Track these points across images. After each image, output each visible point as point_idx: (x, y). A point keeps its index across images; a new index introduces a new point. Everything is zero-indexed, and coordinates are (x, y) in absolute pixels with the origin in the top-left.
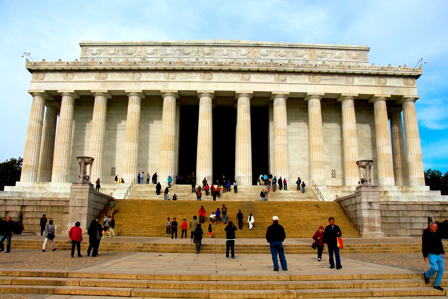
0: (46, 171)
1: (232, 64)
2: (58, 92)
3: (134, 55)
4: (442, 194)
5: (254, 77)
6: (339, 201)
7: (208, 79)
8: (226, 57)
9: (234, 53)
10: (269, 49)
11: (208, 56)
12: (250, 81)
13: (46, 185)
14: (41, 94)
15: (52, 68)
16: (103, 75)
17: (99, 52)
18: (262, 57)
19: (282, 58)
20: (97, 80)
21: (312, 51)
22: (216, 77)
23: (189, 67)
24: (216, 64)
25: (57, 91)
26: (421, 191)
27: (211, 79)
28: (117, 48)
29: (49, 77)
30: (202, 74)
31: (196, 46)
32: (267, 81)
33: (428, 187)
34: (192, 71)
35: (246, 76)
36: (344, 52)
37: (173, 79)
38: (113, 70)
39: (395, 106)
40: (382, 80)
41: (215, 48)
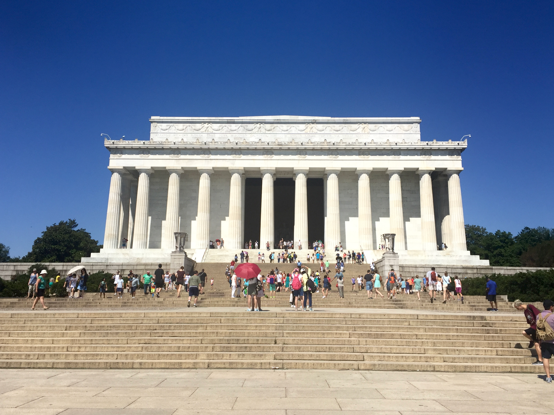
1: (290, 144)
2: (136, 168)
8: (285, 132)
9: (292, 128)
11: (269, 132)
18: (319, 132)
19: (337, 132)
24: (277, 143)
26: (460, 256)
31: (257, 123)
33: (469, 252)
39: (440, 178)
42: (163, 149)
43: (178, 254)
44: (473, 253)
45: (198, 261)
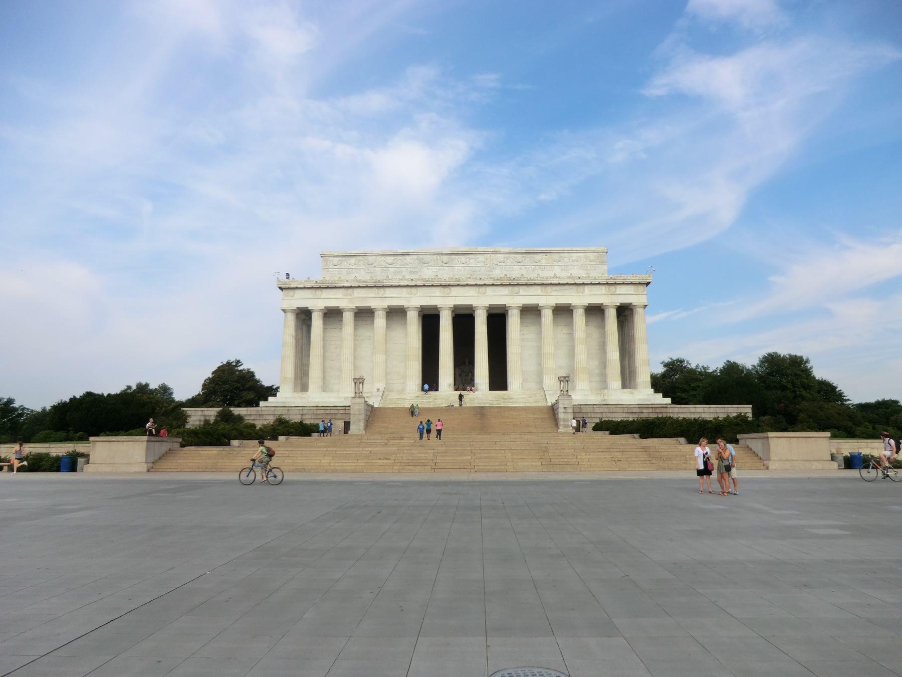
0: (301, 381)
4: (664, 397)
5: (489, 290)
6: (553, 406)
9: (472, 261)
10: (507, 256)
13: (304, 395)
15: (302, 286)
16: (350, 291)
21: (549, 255)
23: (430, 283)
29: (299, 294)
32: (502, 294)
35: (482, 289)
36: (582, 255)
39: (625, 312)
40: (613, 288)
41: (453, 256)
42: (335, 287)
43: (357, 399)
44: (656, 391)
45: (376, 405)
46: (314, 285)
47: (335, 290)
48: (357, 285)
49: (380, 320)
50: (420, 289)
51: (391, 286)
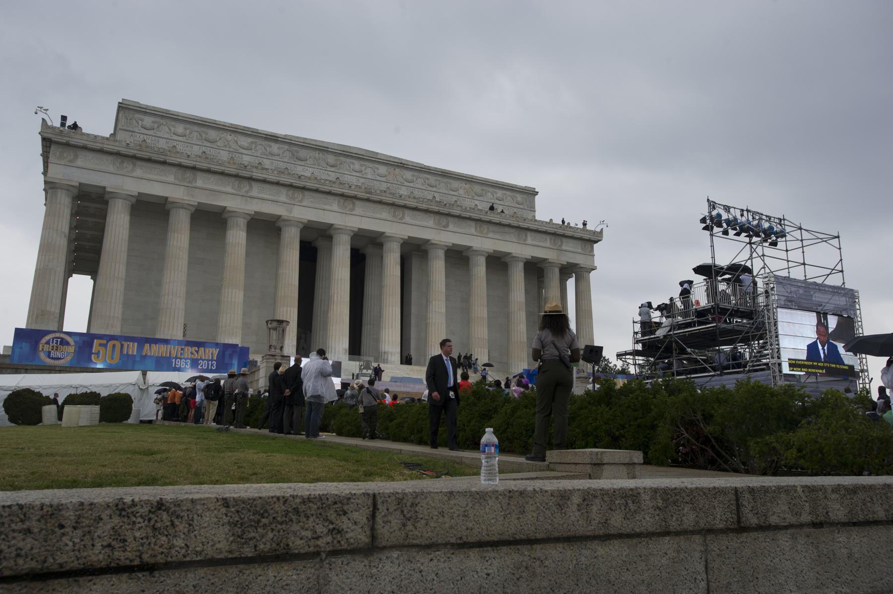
2: (108, 190)
3: (218, 144)
7: (349, 210)
8: (357, 174)
9: (369, 170)
11: (332, 169)
12: (404, 221)
14: (68, 188)
15: (98, 146)
16: (189, 174)
17: (156, 125)
20: (177, 182)
22: (360, 208)
23: (327, 188)
25: (104, 188)
27: (353, 209)
28: (188, 126)
30: (342, 201)
34: (329, 193)
35: (399, 212)
37: (301, 201)
38: (208, 171)
42: (164, 163)
46: (123, 150)
47: (162, 167)
48: (205, 165)
49: (237, 237)
50: (307, 193)
51: (264, 181)
